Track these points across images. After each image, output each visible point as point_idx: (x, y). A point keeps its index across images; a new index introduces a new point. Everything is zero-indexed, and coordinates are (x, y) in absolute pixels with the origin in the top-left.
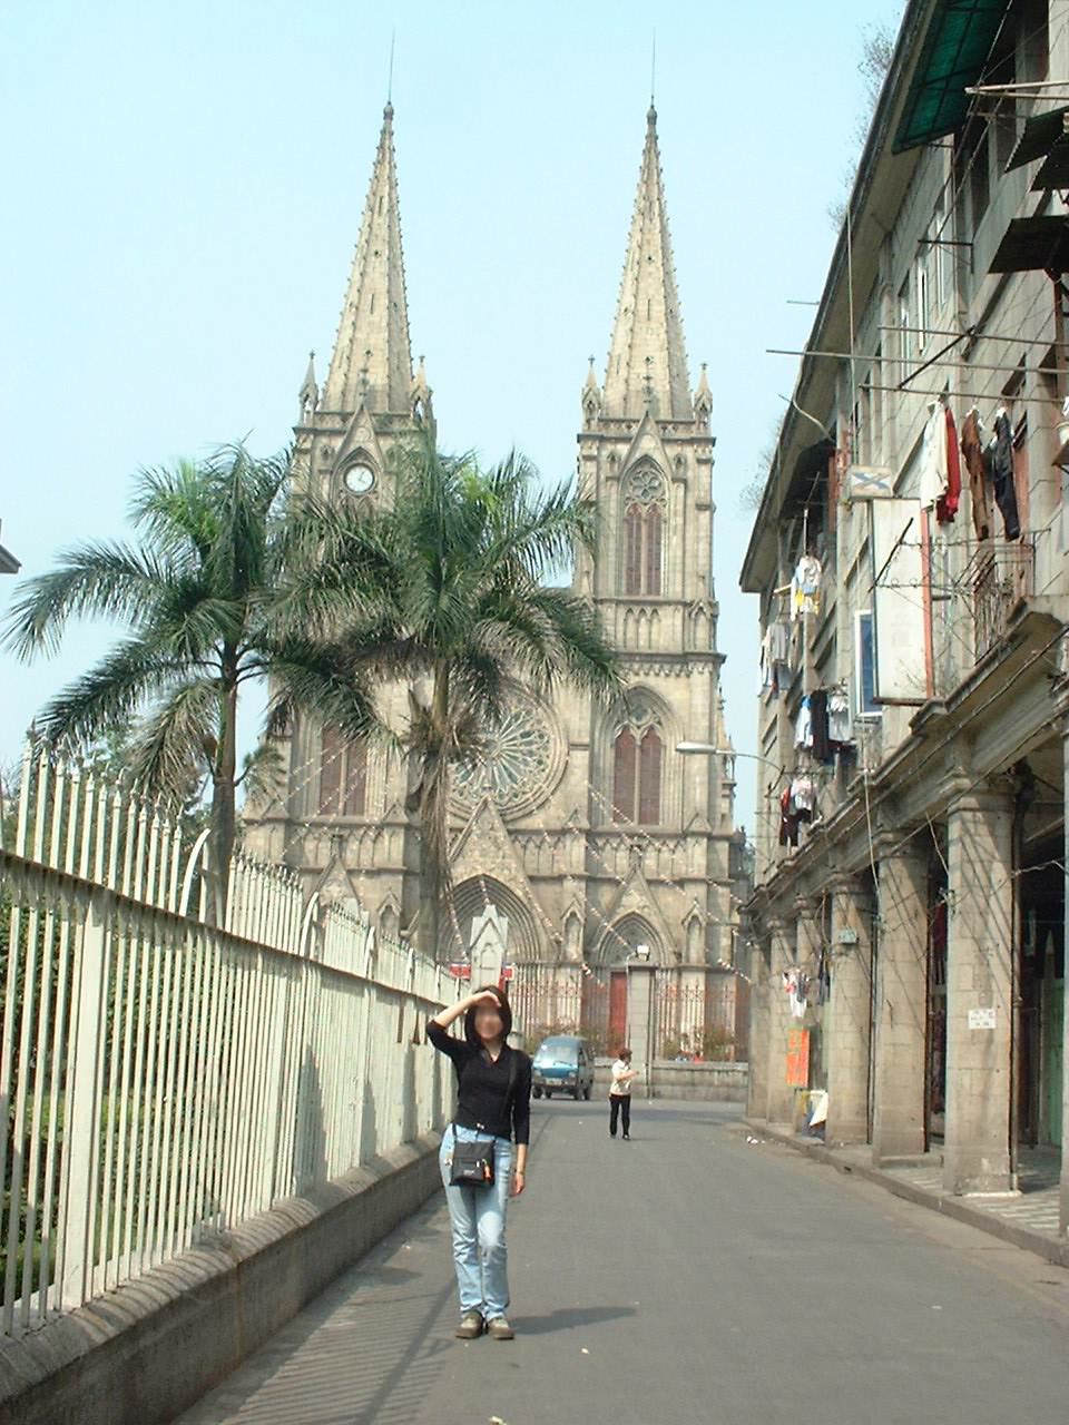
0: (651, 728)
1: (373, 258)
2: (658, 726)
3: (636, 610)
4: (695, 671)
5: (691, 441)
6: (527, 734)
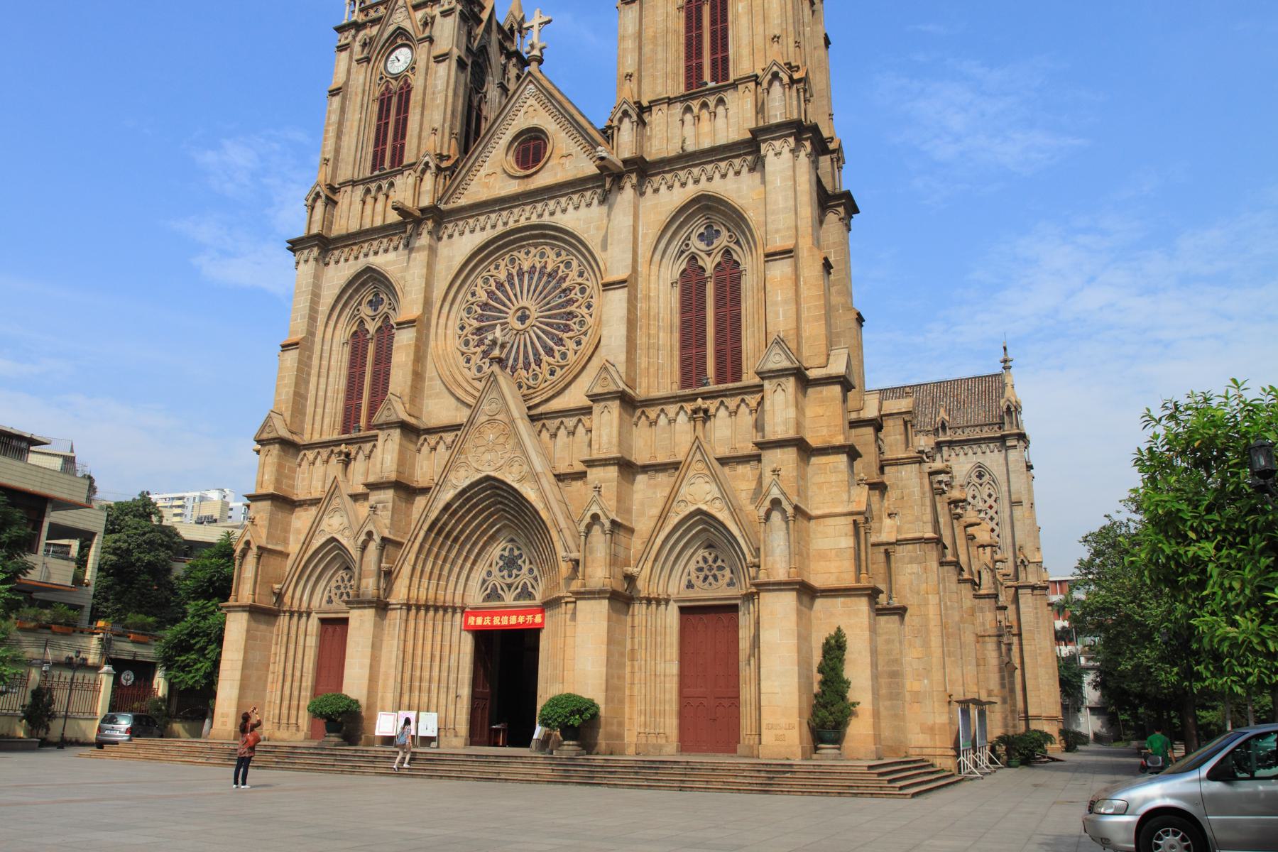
0: (727, 252)
2: (736, 247)
4: (770, 155)
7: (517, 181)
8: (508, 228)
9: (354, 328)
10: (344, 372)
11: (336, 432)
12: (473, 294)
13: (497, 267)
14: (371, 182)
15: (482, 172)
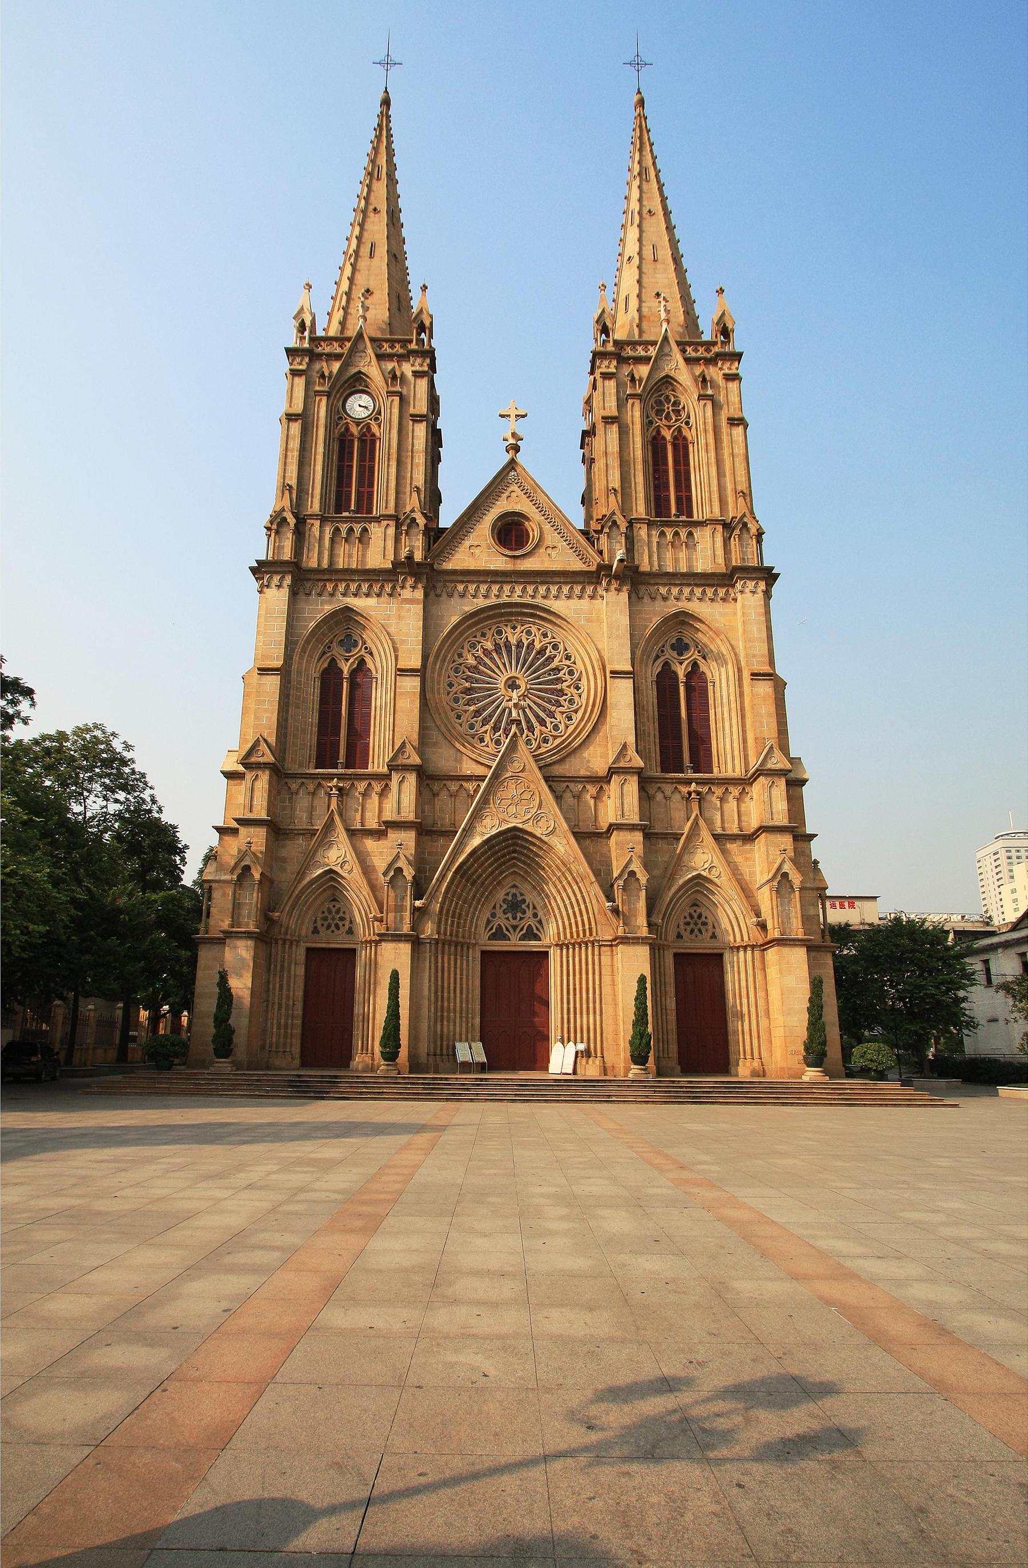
1: (372, 215)
2: (703, 661)
3: (669, 533)
5: (711, 361)
6: (557, 670)
7: (505, 558)
8: (501, 601)
9: (326, 665)
10: (317, 706)
11: (312, 764)
12: (460, 656)
13: (483, 635)
14: (346, 522)
15: (467, 543)
